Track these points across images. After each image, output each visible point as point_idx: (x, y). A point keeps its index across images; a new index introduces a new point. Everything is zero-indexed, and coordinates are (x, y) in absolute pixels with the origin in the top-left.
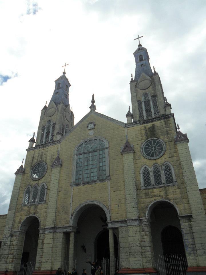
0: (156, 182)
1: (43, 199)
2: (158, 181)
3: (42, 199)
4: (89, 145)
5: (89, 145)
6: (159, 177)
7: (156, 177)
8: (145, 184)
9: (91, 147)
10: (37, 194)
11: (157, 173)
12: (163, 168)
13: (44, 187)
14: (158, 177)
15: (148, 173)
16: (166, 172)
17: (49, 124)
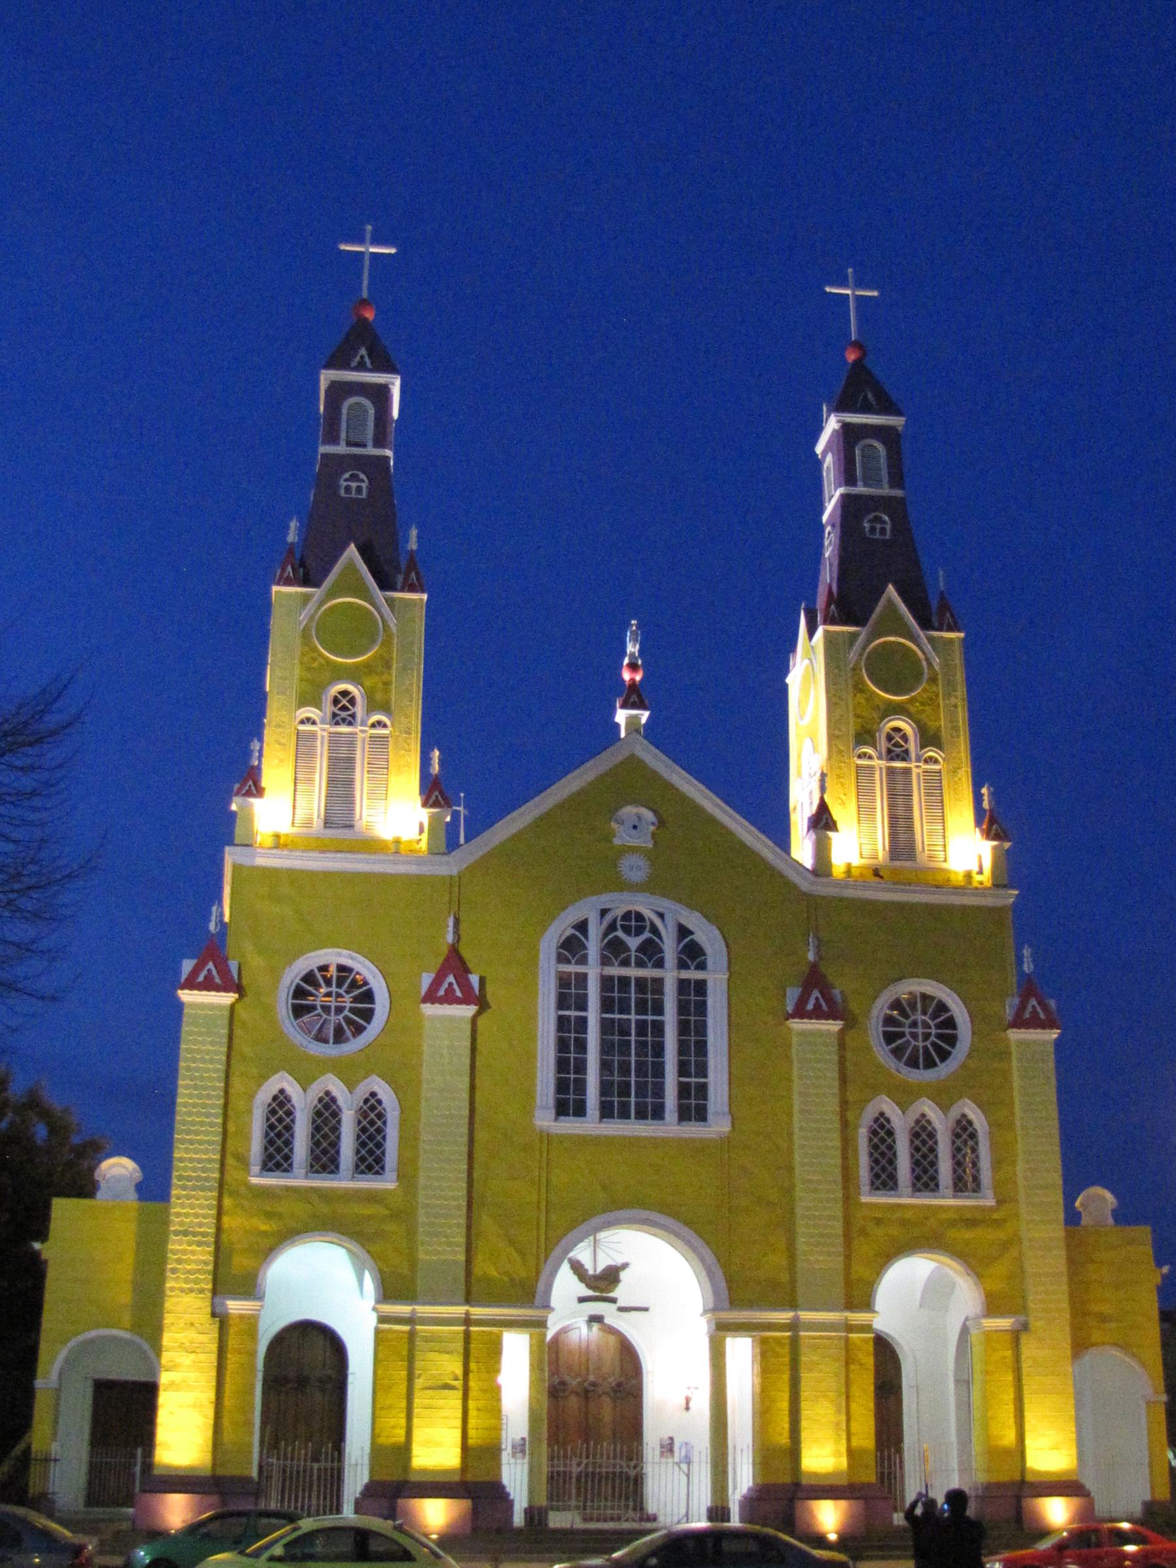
0: (918, 1178)
1: (379, 1160)
2: (925, 1180)
3: (370, 1159)
4: (620, 933)
5: (620, 933)
6: (931, 1157)
7: (918, 1156)
8: (877, 1176)
9: (633, 943)
10: (336, 1129)
11: (924, 1142)
12: (951, 1123)
13: (380, 1102)
14: (924, 1157)
15: (890, 1133)
16: (958, 1142)
17: (344, 708)
